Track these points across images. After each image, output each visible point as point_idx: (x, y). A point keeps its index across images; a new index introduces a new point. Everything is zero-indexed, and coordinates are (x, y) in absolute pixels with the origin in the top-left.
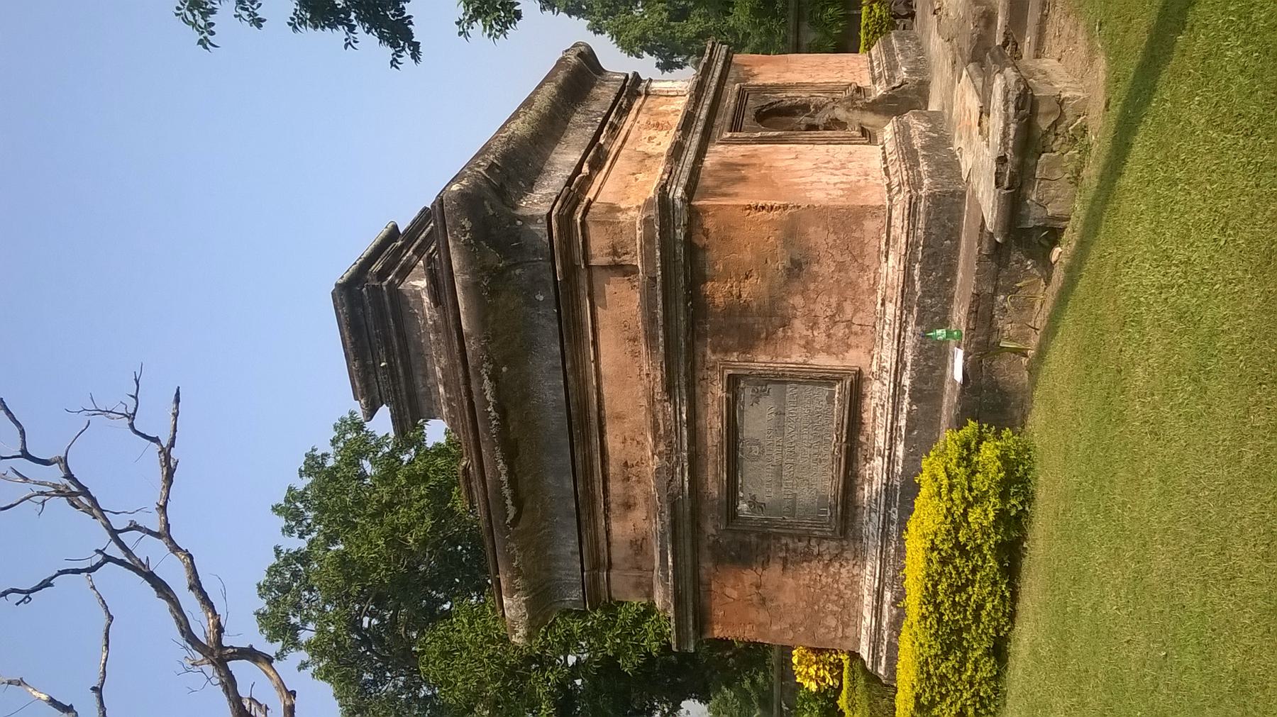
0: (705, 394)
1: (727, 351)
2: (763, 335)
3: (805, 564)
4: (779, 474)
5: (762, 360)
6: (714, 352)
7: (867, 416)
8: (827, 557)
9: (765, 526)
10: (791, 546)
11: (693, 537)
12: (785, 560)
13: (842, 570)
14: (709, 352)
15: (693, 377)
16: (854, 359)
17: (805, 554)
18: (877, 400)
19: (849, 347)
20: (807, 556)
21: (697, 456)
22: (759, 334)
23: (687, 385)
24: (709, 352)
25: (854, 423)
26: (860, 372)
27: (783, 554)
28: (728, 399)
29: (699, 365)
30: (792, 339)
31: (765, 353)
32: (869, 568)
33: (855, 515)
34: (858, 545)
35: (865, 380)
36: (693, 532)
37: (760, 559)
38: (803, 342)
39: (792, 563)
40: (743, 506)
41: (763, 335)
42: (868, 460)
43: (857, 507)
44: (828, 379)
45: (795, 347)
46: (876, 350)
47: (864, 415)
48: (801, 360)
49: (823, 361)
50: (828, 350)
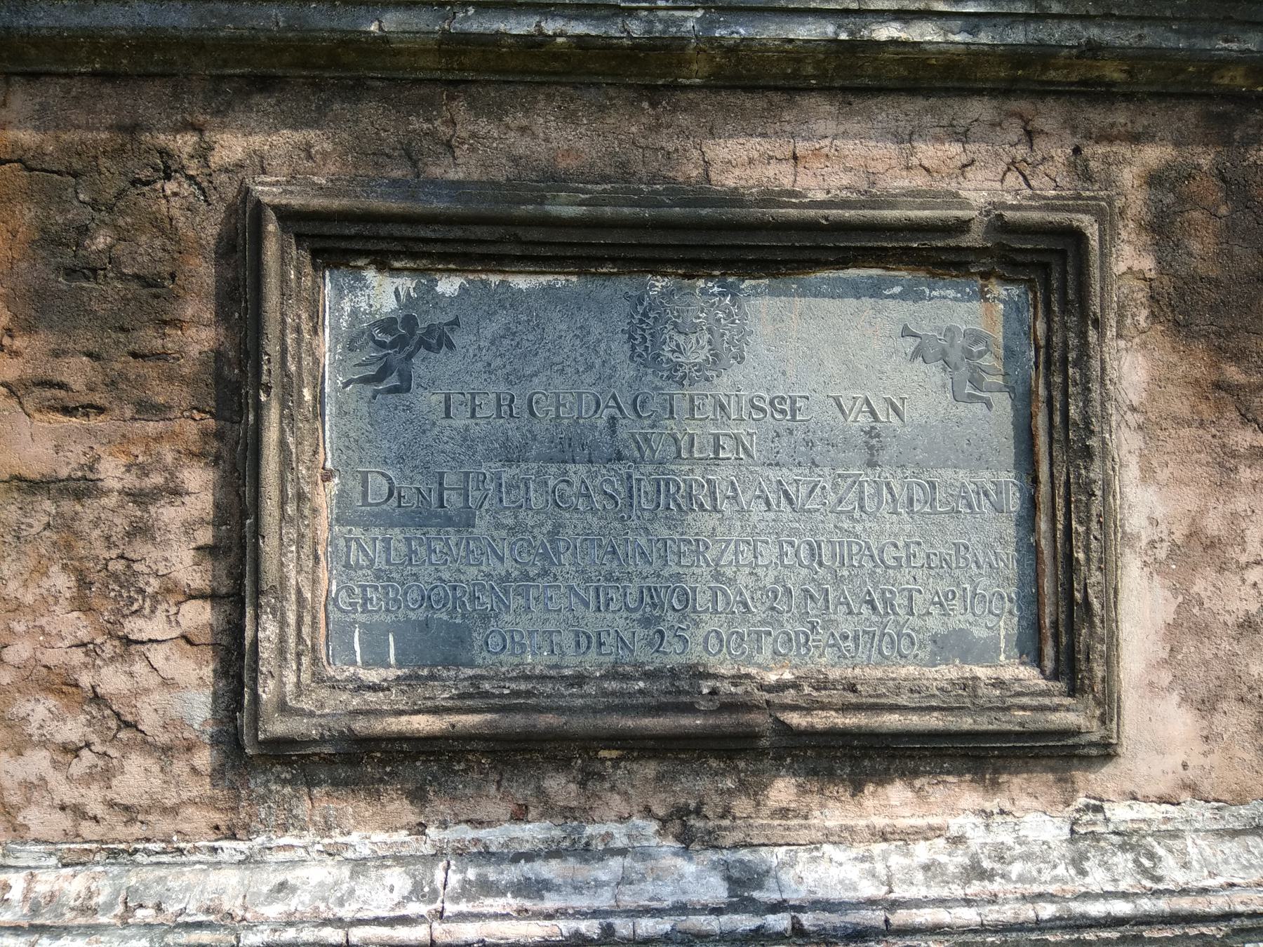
0: (963, 137)
1: (1161, 230)
2: (1233, 373)
3: (62, 582)
4: (567, 449)
5: (1133, 368)
6: (1154, 180)
7: (895, 802)
8: (112, 680)
9: (289, 391)
10: (168, 514)
11: (197, 45)
12: (83, 487)
13: (38, 762)
14: (1154, 155)
15: (1043, 91)
16: (1158, 727)
17: (127, 579)
18: (977, 837)
19: (1206, 705)
20: (109, 591)
21: (652, 93)
22: (1238, 357)
23: (1041, 55)
24: (1154, 155)
25: (859, 755)
26: (1106, 752)
27: (112, 472)
28: (962, 226)
29: (1097, 116)
30: (1224, 481)
31: (1157, 382)
32: (73, 885)
33: (375, 795)
34: (198, 819)
35: (1064, 780)
36: (239, 47)
37: (76, 373)
38: (1214, 525)
39: (66, 526)
40: (383, 292)
41: (1233, 373)
42: (686, 828)
43: (418, 796)
44: (1066, 631)
45: (1190, 500)
46: (1201, 813)
47: (897, 792)
48: (1135, 522)
49: (1140, 611)
50: (1187, 625)
